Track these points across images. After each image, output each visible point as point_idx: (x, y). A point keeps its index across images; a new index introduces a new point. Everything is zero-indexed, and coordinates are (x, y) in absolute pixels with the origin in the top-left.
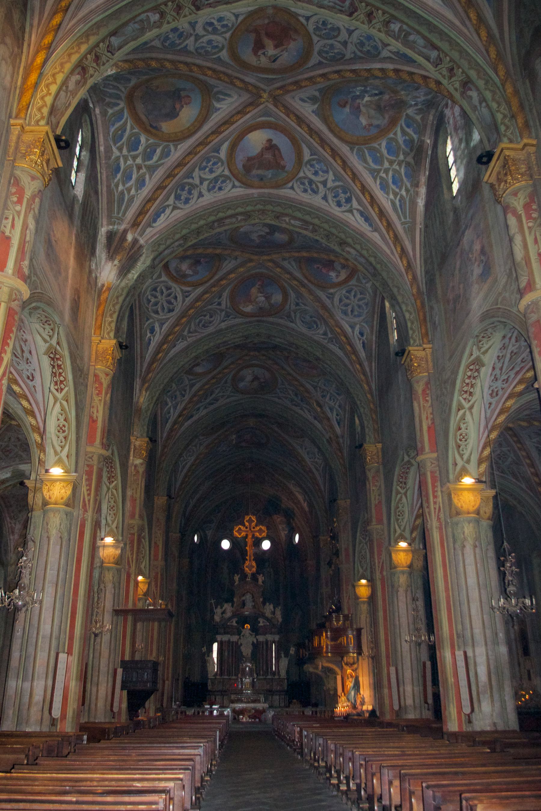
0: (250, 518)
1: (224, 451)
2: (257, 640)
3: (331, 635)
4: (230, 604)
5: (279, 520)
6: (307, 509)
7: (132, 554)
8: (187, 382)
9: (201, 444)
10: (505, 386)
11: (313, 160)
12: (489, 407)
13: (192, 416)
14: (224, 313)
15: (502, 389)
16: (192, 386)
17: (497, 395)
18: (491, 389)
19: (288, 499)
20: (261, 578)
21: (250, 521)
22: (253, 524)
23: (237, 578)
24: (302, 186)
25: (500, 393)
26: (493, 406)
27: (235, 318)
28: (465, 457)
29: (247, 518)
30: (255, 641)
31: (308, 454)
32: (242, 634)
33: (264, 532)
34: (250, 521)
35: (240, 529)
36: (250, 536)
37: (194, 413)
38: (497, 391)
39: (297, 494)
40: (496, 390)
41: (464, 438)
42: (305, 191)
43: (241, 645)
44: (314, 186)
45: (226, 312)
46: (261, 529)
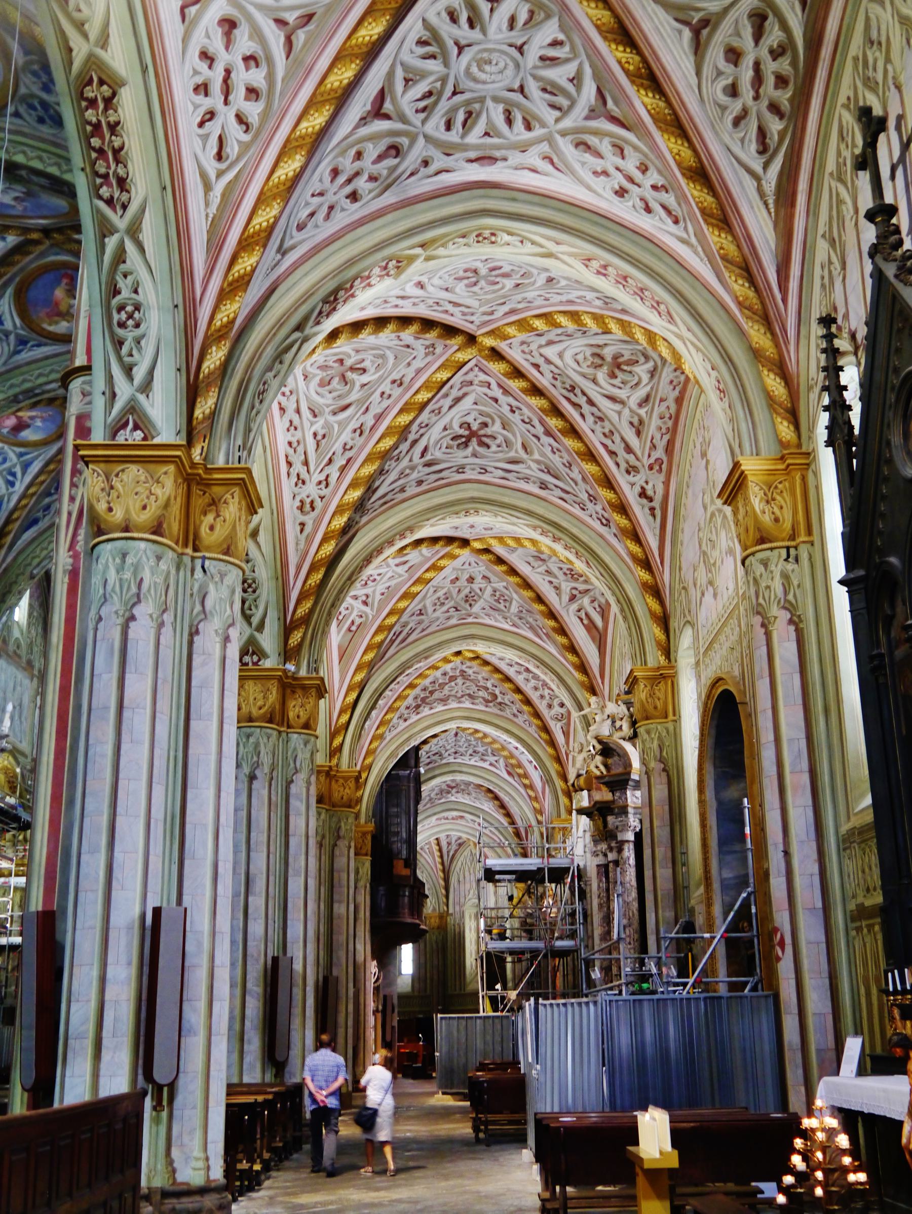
8: (12, 456)
10: (325, 492)
11: (31, 62)
12: (302, 531)
13: (35, 522)
14: (12, 338)
15: (322, 498)
16: (26, 466)
17: (313, 509)
18: (298, 499)
24: (33, 112)
25: (319, 504)
26: (308, 529)
27: (39, 345)
28: (255, 621)
37: (40, 514)
38: (312, 502)
40: (308, 501)
41: (250, 586)
42: (41, 120)
44: (52, 111)
45: (17, 335)
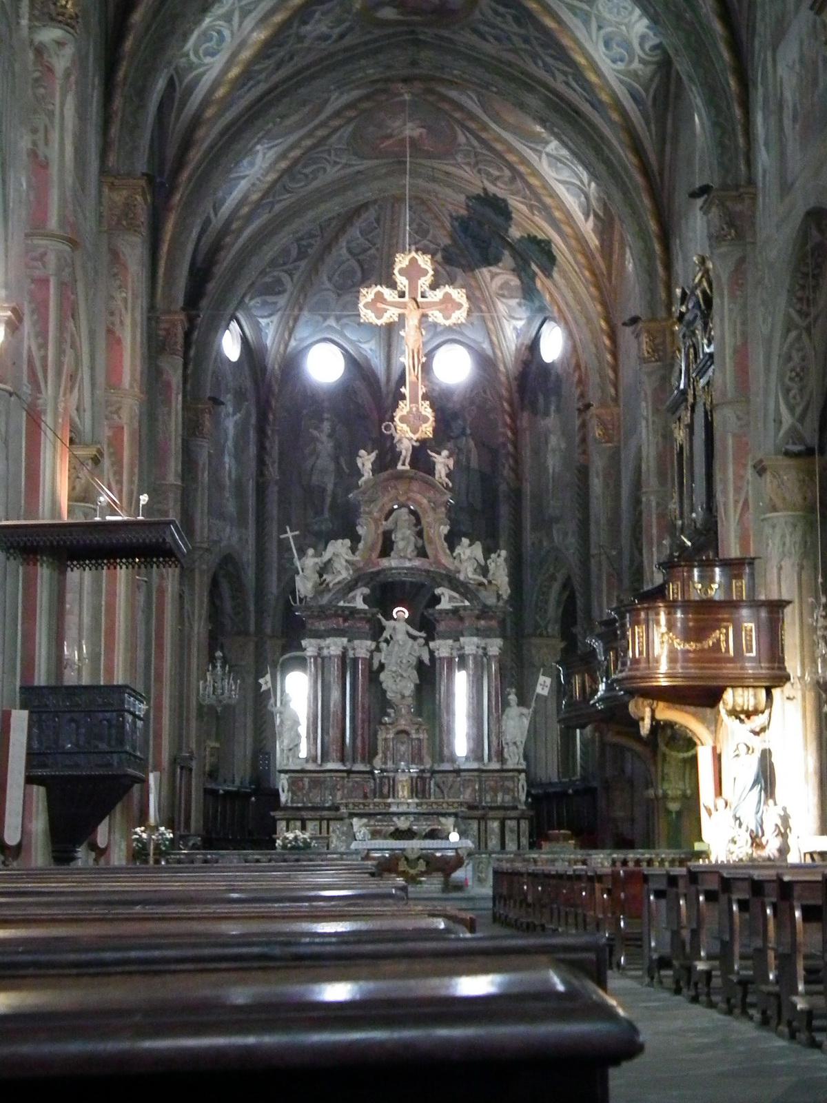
0: (413, 261)
1: (324, 38)
2: (431, 653)
3: (685, 621)
4: (348, 542)
5: (498, 281)
6: (594, 241)
7: (43, 346)
9: (245, 13)
19: (531, 207)
20: (442, 462)
21: (413, 272)
22: (425, 282)
23: (366, 461)
29: (402, 261)
30: (426, 659)
31: (607, 45)
32: (386, 634)
33: (459, 306)
34: (413, 272)
35: (379, 297)
36: (413, 320)
39: (561, 190)
43: (382, 667)
46: (448, 296)
